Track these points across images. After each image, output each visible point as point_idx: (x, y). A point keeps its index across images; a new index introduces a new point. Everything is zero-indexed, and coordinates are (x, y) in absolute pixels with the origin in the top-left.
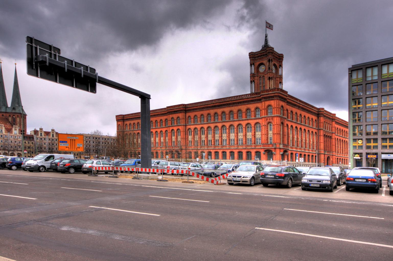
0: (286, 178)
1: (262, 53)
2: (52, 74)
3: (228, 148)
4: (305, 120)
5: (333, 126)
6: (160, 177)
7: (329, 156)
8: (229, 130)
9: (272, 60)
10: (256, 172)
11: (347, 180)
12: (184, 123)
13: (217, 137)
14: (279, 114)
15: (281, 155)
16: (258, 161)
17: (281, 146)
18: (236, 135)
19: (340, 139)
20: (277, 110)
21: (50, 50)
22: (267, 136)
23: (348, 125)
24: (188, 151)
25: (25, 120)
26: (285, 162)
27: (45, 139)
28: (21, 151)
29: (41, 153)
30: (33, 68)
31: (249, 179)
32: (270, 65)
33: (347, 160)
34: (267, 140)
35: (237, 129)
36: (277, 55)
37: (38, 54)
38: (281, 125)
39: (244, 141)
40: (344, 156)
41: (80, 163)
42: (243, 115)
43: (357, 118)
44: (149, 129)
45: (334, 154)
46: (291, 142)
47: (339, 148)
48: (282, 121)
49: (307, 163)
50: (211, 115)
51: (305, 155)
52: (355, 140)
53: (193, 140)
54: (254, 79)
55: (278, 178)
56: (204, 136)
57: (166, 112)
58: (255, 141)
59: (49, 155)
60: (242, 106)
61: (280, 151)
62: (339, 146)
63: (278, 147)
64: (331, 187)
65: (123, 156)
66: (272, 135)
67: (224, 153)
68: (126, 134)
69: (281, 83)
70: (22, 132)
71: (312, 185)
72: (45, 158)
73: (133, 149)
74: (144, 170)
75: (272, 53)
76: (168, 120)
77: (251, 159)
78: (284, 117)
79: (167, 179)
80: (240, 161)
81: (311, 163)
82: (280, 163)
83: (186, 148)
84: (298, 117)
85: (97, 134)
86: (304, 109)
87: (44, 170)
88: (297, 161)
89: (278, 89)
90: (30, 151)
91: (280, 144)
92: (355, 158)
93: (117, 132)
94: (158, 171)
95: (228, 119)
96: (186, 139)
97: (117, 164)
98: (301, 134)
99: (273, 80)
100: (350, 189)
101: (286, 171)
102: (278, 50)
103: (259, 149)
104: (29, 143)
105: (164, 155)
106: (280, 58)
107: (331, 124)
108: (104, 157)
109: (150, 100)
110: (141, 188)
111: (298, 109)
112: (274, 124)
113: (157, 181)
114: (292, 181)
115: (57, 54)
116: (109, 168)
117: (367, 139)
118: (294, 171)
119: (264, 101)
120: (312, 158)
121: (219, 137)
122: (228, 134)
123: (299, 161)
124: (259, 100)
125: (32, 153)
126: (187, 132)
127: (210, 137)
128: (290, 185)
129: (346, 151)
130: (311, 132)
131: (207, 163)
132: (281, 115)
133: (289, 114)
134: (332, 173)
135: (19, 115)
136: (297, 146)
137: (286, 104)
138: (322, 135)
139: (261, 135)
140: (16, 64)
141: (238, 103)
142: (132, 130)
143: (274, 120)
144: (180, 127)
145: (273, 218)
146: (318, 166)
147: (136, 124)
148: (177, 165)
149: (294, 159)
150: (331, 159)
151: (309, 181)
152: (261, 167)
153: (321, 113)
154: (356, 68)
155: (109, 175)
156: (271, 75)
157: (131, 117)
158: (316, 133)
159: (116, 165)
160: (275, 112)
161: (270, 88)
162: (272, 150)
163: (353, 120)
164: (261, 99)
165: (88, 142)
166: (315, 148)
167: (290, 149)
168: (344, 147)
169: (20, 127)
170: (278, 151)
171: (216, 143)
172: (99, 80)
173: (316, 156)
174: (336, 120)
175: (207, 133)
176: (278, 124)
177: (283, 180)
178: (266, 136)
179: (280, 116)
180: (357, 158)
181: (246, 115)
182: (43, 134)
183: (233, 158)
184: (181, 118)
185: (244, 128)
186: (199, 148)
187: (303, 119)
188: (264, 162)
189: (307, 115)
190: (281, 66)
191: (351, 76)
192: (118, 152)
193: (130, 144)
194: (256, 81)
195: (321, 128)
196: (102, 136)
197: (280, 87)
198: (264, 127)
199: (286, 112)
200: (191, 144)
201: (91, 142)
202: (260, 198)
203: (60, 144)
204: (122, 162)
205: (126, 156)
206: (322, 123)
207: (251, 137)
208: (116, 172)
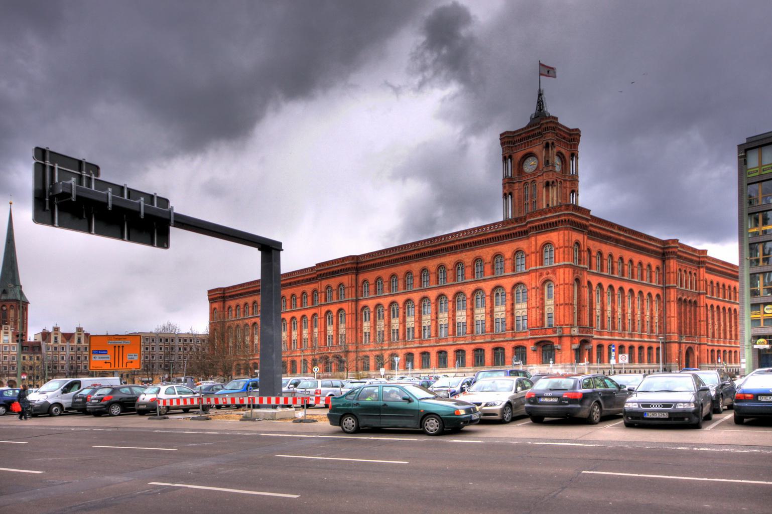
0: (588, 402)
1: (528, 132)
2: (81, 218)
3: (451, 343)
4: (633, 270)
5: (702, 279)
6: (300, 414)
7: (691, 345)
8: (454, 302)
9: (553, 143)
10: (516, 392)
11: (738, 400)
12: (354, 295)
13: (427, 320)
14: (569, 261)
15: (573, 352)
16: (521, 368)
17: (575, 331)
18: (469, 312)
19: (718, 307)
20: (564, 252)
21: (80, 170)
22: (541, 312)
23: (737, 272)
24: (361, 354)
25: (25, 312)
26: (584, 365)
27: (63, 348)
28: (16, 375)
29: (54, 377)
30: (44, 209)
31: (499, 407)
32: (549, 156)
33: (736, 352)
34: (542, 319)
35: (473, 300)
36: (564, 131)
37: (56, 180)
38: (573, 285)
39: (488, 324)
40: (728, 345)
41: (132, 393)
42: (486, 269)
43: (760, 255)
44: (279, 313)
45: (704, 340)
46: (598, 320)
47: (716, 327)
49: (637, 365)
50: (414, 273)
51: (631, 348)
52: (755, 306)
53: (372, 332)
54: (511, 190)
55: (567, 402)
56: (397, 321)
57: (315, 275)
58: (513, 323)
59: (70, 380)
60: (484, 249)
61: (572, 343)
62: (716, 322)
63: (566, 333)
64: (698, 416)
65: (222, 374)
66: (553, 307)
67: (442, 355)
68: (229, 327)
69: (574, 191)
70: (19, 338)
71: (649, 415)
72: (62, 388)
73: (242, 358)
74: (265, 401)
75: (554, 129)
76: (319, 291)
77: (504, 364)
78: (582, 266)
79: (315, 418)
80: (478, 369)
81: (647, 364)
82: (573, 369)
83: (357, 348)
84: (615, 265)
85: (169, 331)
86: (629, 246)
87: (59, 412)
88: (613, 361)
89: (568, 206)
90: (33, 375)
91: (572, 326)
92: (755, 347)
93: (210, 324)
94: (295, 401)
95: (452, 280)
96: (357, 329)
97: (209, 392)
98: (623, 302)
99: (555, 188)
100: (745, 420)
101: (587, 385)
102: (567, 121)
103: (522, 340)
104: (31, 358)
105: (309, 365)
106: (572, 137)
107: (695, 274)
108: (183, 379)
109: (281, 252)
110: (257, 440)
111: (615, 246)
112: (557, 283)
113: (293, 422)
114: (600, 407)
115: (93, 177)
116: (192, 400)
118: (606, 386)
119: (535, 235)
120: (649, 354)
121: (432, 320)
122: (450, 312)
123: (617, 361)
124: (524, 234)
125: (38, 378)
126: (359, 315)
127: (411, 322)
128: (596, 416)
129: (733, 333)
130: (645, 295)
131: (403, 378)
132: (574, 262)
133: (594, 260)
134: (698, 386)
135: (14, 304)
136: (614, 328)
138: (672, 299)
140: (11, 204)
141: (475, 243)
142: (242, 317)
143: (558, 274)
144: (344, 306)
145: (555, 493)
146: (665, 370)
147: (250, 305)
148: (337, 387)
149: (606, 358)
150: (696, 353)
151: (643, 406)
152: (528, 381)
153: (670, 250)
154: (757, 144)
155: (191, 416)
156: (551, 176)
157: (239, 292)
158: (658, 296)
159: (206, 394)
160: (561, 256)
161: (548, 205)
163: (751, 262)
164: (527, 231)
165: (150, 349)
166: (656, 330)
167: (595, 336)
168: (728, 324)
169: (16, 328)
170: (566, 342)
171: (424, 333)
172: (175, 221)
173: (658, 349)
174: (709, 263)
175: (404, 313)
176: (567, 281)
177: (579, 406)
178: (538, 311)
179: (572, 263)
180: (761, 347)
181: (493, 268)
182: (59, 339)
183: (463, 364)
184: (347, 285)
185: (487, 296)
186: (386, 347)
187: (626, 267)
188: (535, 369)
189: (637, 258)
191: (745, 162)
192: (211, 365)
193: (236, 348)
194: (516, 193)
195: (671, 285)
196: (178, 334)
197: (573, 201)
198: (534, 291)
199: (585, 255)
200: (369, 339)
201: (157, 348)
202: (525, 450)
203: (94, 356)
204: (219, 387)
205: (227, 374)
206: (673, 272)
207: (503, 316)
208: (205, 408)
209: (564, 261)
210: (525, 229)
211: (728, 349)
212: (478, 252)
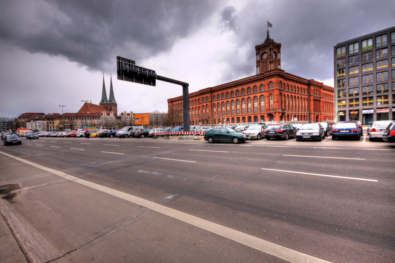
0: (284, 133)
1: (264, 45)
2: (130, 78)
3: (241, 115)
4: (299, 90)
5: (321, 92)
6: (196, 137)
7: (318, 115)
8: (241, 102)
9: (272, 48)
10: (262, 130)
11: (333, 132)
12: (211, 100)
13: (233, 107)
14: (278, 87)
15: (280, 117)
16: (263, 122)
17: (280, 111)
18: (246, 105)
19: (327, 102)
20: (276, 84)
21: (130, 63)
23: (333, 90)
24: (213, 119)
26: (283, 121)
27: (127, 118)
28: (115, 126)
30: (120, 75)
31: (256, 135)
32: (271, 53)
33: (333, 117)
34: (269, 107)
35: (247, 101)
36: (276, 44)
37: (123, 66)
38: (279, 95)
39: (252, 109)
40: (330, 114)
41: (147, 131)
43: (341, 84)
44: (188, 106)
45: (322, 112)
47: (326, 108)
48: (280, 92)
49: (300, 121)
50: (229, 93)
51: (298, 116)
52: (339, 101)
53: (217, 111)
54: (259, 65)
55: (278, 133)
56: (224, 108)
57: (199, 94)
58: (260, 108)
59: (130, 127)
61: (279, 114)
62: (326, 107)
63: (277, 111)
64: (320, 137)
65: (172, 125)
66: (273, 103)
67: (238, 118)
68: (174, 111)
69: (279, 64)
70: (115, 115)
71: (304, 137)
72: (128, 129)
73: (178, 120)
74: (185, 133)
75: (272, 43)
77: (257, 121)
78: (282, 89)
79: (200, 138)
80: (250, 123)
82: (279, 123)
83: (212, 117)
84: (293, 88)
85: (157, 112)
86: (297, 82)
87: (127, 137)
88: (292, 120)
89: (277, 69)
90: (120, 126)
91: (279, 109)
92: (339, 114)
93: (168, 110)
94: (194, 133)
96: (212, 111)
97: (169, 131)
98: (296, 101)
99: (273, 64)
100: (336, 138)
101: (284, 128)
102: (277, 41)
103: (263, 113)
104: (119, 121)
105: (198, 122)
106: (278, 46)
108: (161, 127)
109: (189, 86)
110: (183, 145)
111: (293, 82)
112: (274, 95)
115: (133, 65)
116: (164, 133)
117: (350, 100)
118: (290, 128)
120: (304, 118)
121: (235, 107)
122: (240, 105)
123: (294, 120)
124: (263, 79)
125: (121, 127)
126: (212, 106)
127: (228, 108)
128: (287, 138)
129: (332, 110)
130: (303, 98)
131: (226, 126)
133: (286, 87)
134: (320, 127)
135: (113, 105)
136: (292, 109)
137: (283, 79)
138: (312, 99)
139: (265, 103)
140: (111, 74)
141: (248, 82)
142: (178, 107)
143: (274, 92)
144: (208, 103)
145: (274, 161)
146: (309, 123)
147: (180, 104)
148: (206, 129)
149: (290, 119)
150: (320, 117)
151: (302, 134)
152: (265, 126)
153: (311, 83)
154: (340, 46)
155: (164, 138)
156: (272, 60)
157: (176, 100)
158: (307, 98)
159: (168, 131)
160: (275, 86)
161: (271, 69)
162: (273, 113)
163: (338, 86)
165: (151, 118)
166: (306, 110)
167: (287, 112)
168: (330, 107)
169: (114, 112)
170: (277, 114)
171: (233, 112)
172: (157, 78)
173: (307, 116)
174: (324, 87)
175: (226, 105)
176: (277, 94)
177: (281, 134)
179: (279, 88)
181: (254, 90)
182: (126, 115)
183: (245, 122)
184: (208, 97)
186: (221, 116)
187: (296, 89)
188: (267, 123)
189: (300, 86)
190: (279, 52)
191: (336, 52)
192: (169, 123)
193: (176, 117)
194: (260, 66)
195: (311, 94)
197: (279, 67)
198: (267, 97)
199: (283, 85)
200: (216, 114)
201: (153, 118)
202: (265, 148)
203: (136, 120)
204: (172, 129)
205: (174, 125)
206: (312, 90)
207: (257, 106)
208: (168, 136)
209: (276, 87)
210: (264, 77)
211: (330, 116)
212: (249, 85)
